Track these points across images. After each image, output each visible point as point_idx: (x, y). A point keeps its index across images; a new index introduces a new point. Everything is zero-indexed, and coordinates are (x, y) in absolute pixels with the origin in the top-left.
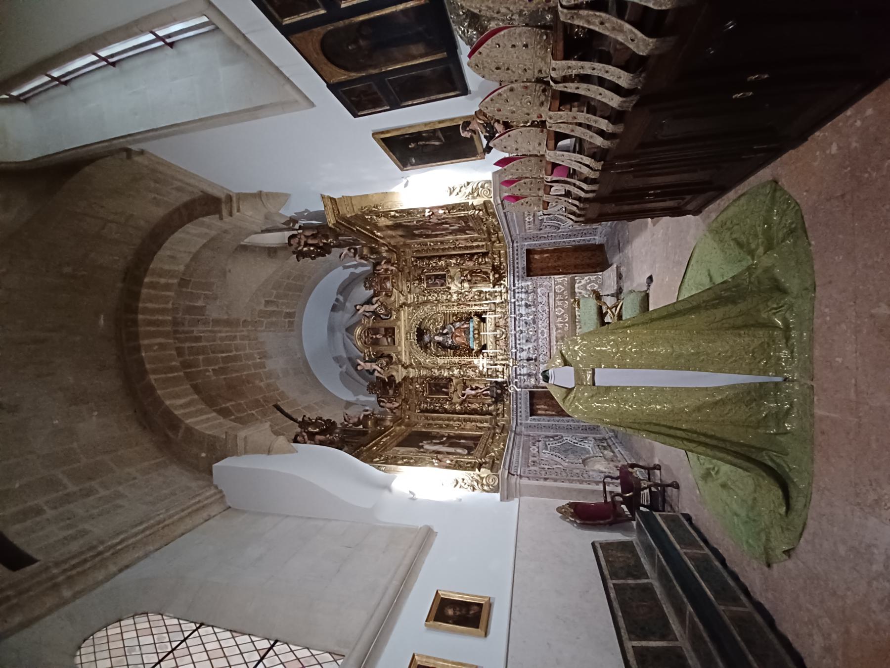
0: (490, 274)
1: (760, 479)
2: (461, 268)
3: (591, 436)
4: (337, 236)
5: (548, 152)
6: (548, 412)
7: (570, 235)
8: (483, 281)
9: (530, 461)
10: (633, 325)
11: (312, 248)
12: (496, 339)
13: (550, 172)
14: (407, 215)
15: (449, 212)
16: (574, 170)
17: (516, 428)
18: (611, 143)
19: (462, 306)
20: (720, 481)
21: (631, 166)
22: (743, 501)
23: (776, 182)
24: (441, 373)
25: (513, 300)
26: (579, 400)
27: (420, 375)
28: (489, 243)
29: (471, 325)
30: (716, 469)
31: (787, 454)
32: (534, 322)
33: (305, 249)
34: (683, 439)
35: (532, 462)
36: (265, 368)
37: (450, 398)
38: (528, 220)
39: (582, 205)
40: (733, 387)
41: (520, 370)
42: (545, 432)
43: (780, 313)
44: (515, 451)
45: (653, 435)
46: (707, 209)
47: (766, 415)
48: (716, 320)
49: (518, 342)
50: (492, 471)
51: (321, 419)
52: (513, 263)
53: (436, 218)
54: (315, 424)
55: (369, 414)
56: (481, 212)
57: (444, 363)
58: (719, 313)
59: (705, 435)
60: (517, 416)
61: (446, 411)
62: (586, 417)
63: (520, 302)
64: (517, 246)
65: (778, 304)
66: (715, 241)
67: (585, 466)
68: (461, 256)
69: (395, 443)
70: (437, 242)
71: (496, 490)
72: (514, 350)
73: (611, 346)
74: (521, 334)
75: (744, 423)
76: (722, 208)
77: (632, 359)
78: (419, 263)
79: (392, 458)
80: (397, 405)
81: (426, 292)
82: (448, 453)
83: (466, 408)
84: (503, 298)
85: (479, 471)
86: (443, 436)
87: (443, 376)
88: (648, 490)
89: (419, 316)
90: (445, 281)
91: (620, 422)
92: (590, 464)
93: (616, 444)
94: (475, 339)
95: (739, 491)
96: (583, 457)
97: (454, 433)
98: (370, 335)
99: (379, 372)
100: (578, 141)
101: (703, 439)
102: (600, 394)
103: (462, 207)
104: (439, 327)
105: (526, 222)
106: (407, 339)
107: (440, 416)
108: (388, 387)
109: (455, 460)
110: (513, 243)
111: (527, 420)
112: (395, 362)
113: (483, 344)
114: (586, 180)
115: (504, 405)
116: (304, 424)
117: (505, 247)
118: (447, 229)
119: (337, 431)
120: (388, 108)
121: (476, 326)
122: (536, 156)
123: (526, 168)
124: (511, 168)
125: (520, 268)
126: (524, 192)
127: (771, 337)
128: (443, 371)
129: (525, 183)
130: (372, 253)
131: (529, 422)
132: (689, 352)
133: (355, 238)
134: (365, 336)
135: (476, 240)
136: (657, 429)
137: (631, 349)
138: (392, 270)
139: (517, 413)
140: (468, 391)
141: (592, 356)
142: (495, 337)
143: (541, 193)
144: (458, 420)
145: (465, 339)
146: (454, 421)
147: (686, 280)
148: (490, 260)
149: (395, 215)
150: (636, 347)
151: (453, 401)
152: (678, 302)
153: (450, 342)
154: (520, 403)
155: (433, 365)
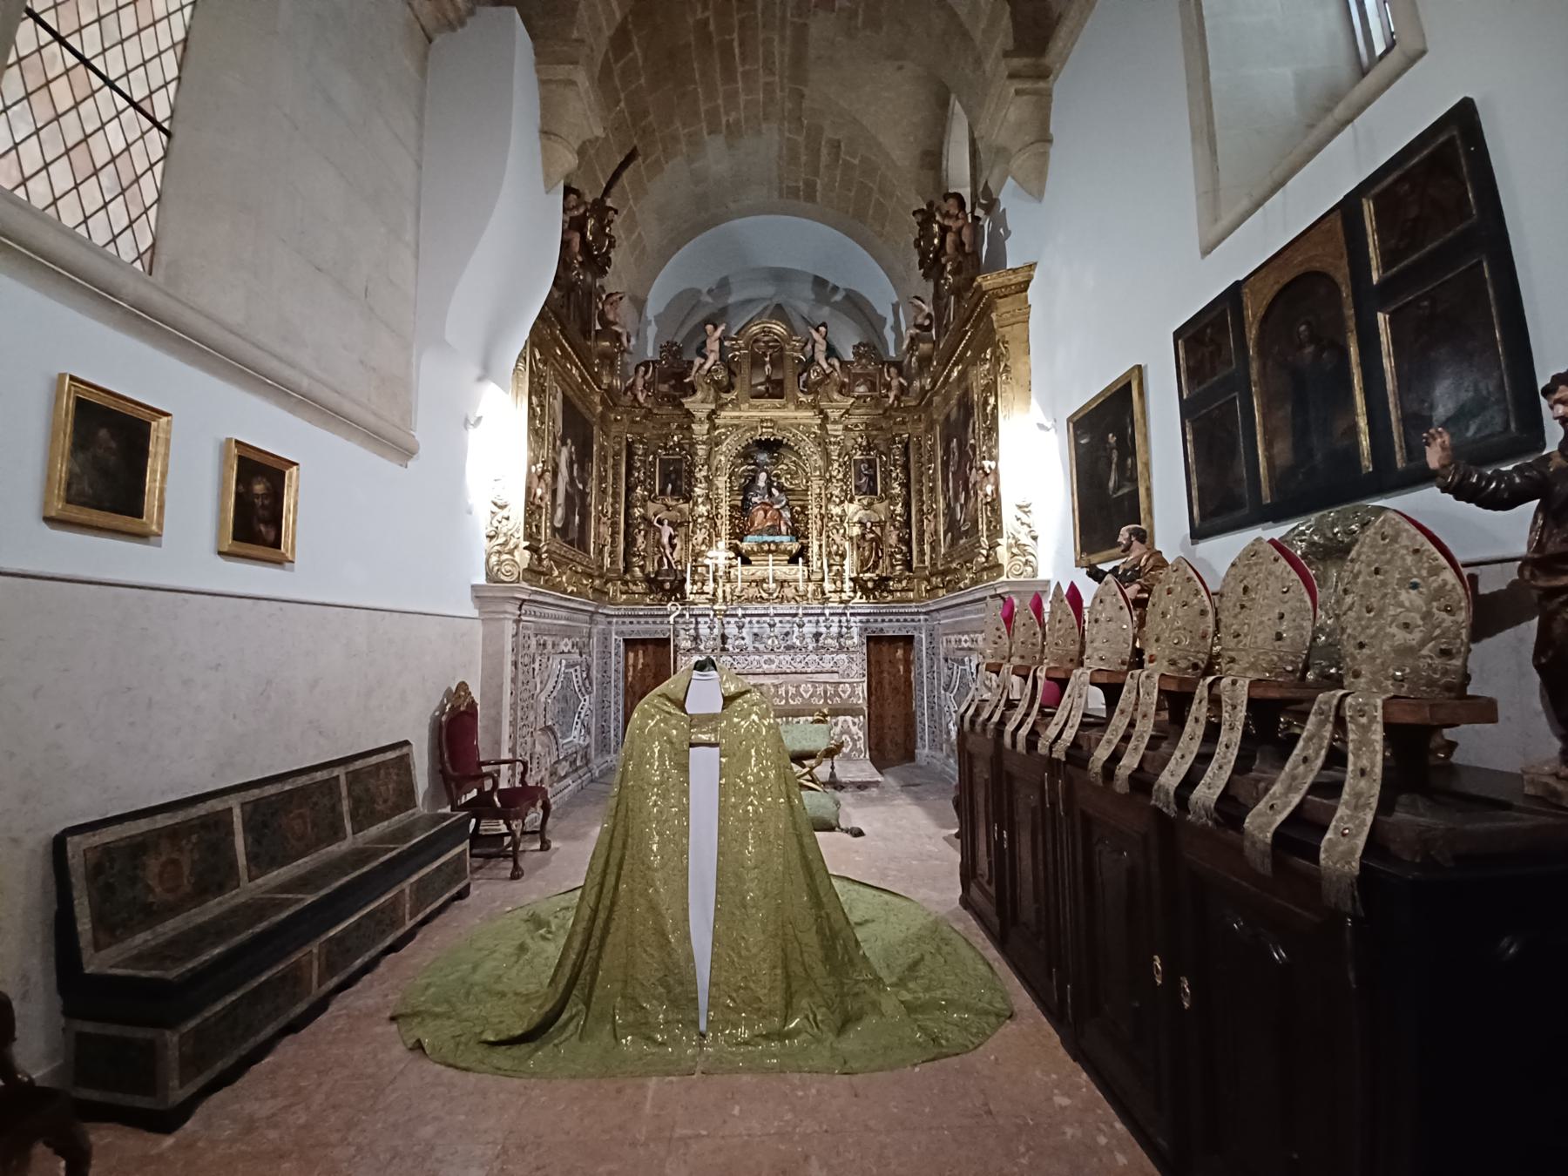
0: (873, 572)
1: (538, 1003)
2: (885, 522)
3: (591, 740)
4: (958, 292)
5: (1089, 672)
6: (631, 669)
7: (932, 708)
8: (862, 561)
9: (545, 638)
10: (792, 807)
11: (936, 241)
12: (760, 582)
13: (1052, 675)
14: (987, 427)
15: (987, 503)
16: (1053, 715)
17: (602, 614)
18: (1096, 773)
19: (820, 523)
20: (529, 941)
21: (1054, 804)
22: (500, 977)
23: (1010, 1017)
24: (701, 482)
25: (827, 612)
26: (664, 720)
27: (697, 443)
28: (927, 572)
29: (785, 539)
30: (550, 936)
31: (581, 1039)
32: (788, 648)
33: (936, 227)
34: (602, 885)
35: (545, 641)
36: (709, 134)
37: (655, 497)
38: (963, 639)
39: (992, 727)
40: (690, 958)
41: (706, 623)
42: (597, 664)
43: (807, 1025)
44: (563, 613)
45: (607, 838)
46: (971, 917)
47: (644, 1008)
48: (800, 934)
49: (755, 619)
50: (524, 570)
52: (892, 614)
53: (978, 479)
54: (600, 231)
55: (621, 344)
56: (983, 559)
57: (717, 489)
58: (811, 939)
59: (609, 920)
60: (624, 616)
61: (630, 489)
62: (634, 732)
63: (823, 624)
64: (919, 620)
65: (822, 1021)
66: (920, 929)
67: (540, 730)
68: (907, 524)
69: (570, 393)
70: (934, 481)
71: (492, 577)
72: (740, 612)
73: (758, 772)
74: (769, 624)
75: (632, 976)
76: (972, 940)
77: (735, 806)
78: (897, 449)
79: (542, 385)
80: (641, 398)
81: (847, 458)
82: (554, 493)
84: (832, 595)
85: (525, 548)
86: (585, 485)
87: (695, 486)
88: (506, 831)
89: (803, 444)
90: (865, 494)
91: (627, 787)
92: (544, 738)
93: (580, 781)
94: (760, 544)
95: (514, 971)
96: (556, 728)
97: (590, 505)
98: (771, 351)
99: (701, 366)
100: (1103, 721)
101: (602, 915)
102: (676, 754)
103: (995, 527)
104: (783, 480)
105: (960, 636)
106: (762, 421)
107: (621, 479)
108: (673, 382)
109: (544, 505)
110: (925, 613)
111: (616, 634)
112: (721, 397)
113: (751, 558)
114: (1034, 734)
116: (600, 210)
117: (919, 600)
118: (957, 498)
119: (589, 279)
120: (1185, 397)
121: (782, 547)
122: (1082, 652)
123: (1062, 636)
124: (1063, 611)
125: (881, 625)
126: (1020, 635)
127: (771, 1013)
128: (703, 485)
129: (1034, 634)
130: (920, 360)
131: (614, 637)
132: (748, 892)
133: (951, 327)
134: (768, 342)
135: (933, 549)
136: (618, 843)
137: (751, 804)
138: (887, 397)
139: (630, 616)
140: (667, 531)
141: (741, 744)
142: (764, 581)
143: (1016, 660)
144: (615, 513)
145: (760, 527)
146: (612, 505)
147: (856, 887)
148: (898, 573)
149: (989, 404)
150: (756, 811)
151: (649, 503)
152: (829, 876)
153: (755, 499)
154: (647, 623)
155: (714, 469)
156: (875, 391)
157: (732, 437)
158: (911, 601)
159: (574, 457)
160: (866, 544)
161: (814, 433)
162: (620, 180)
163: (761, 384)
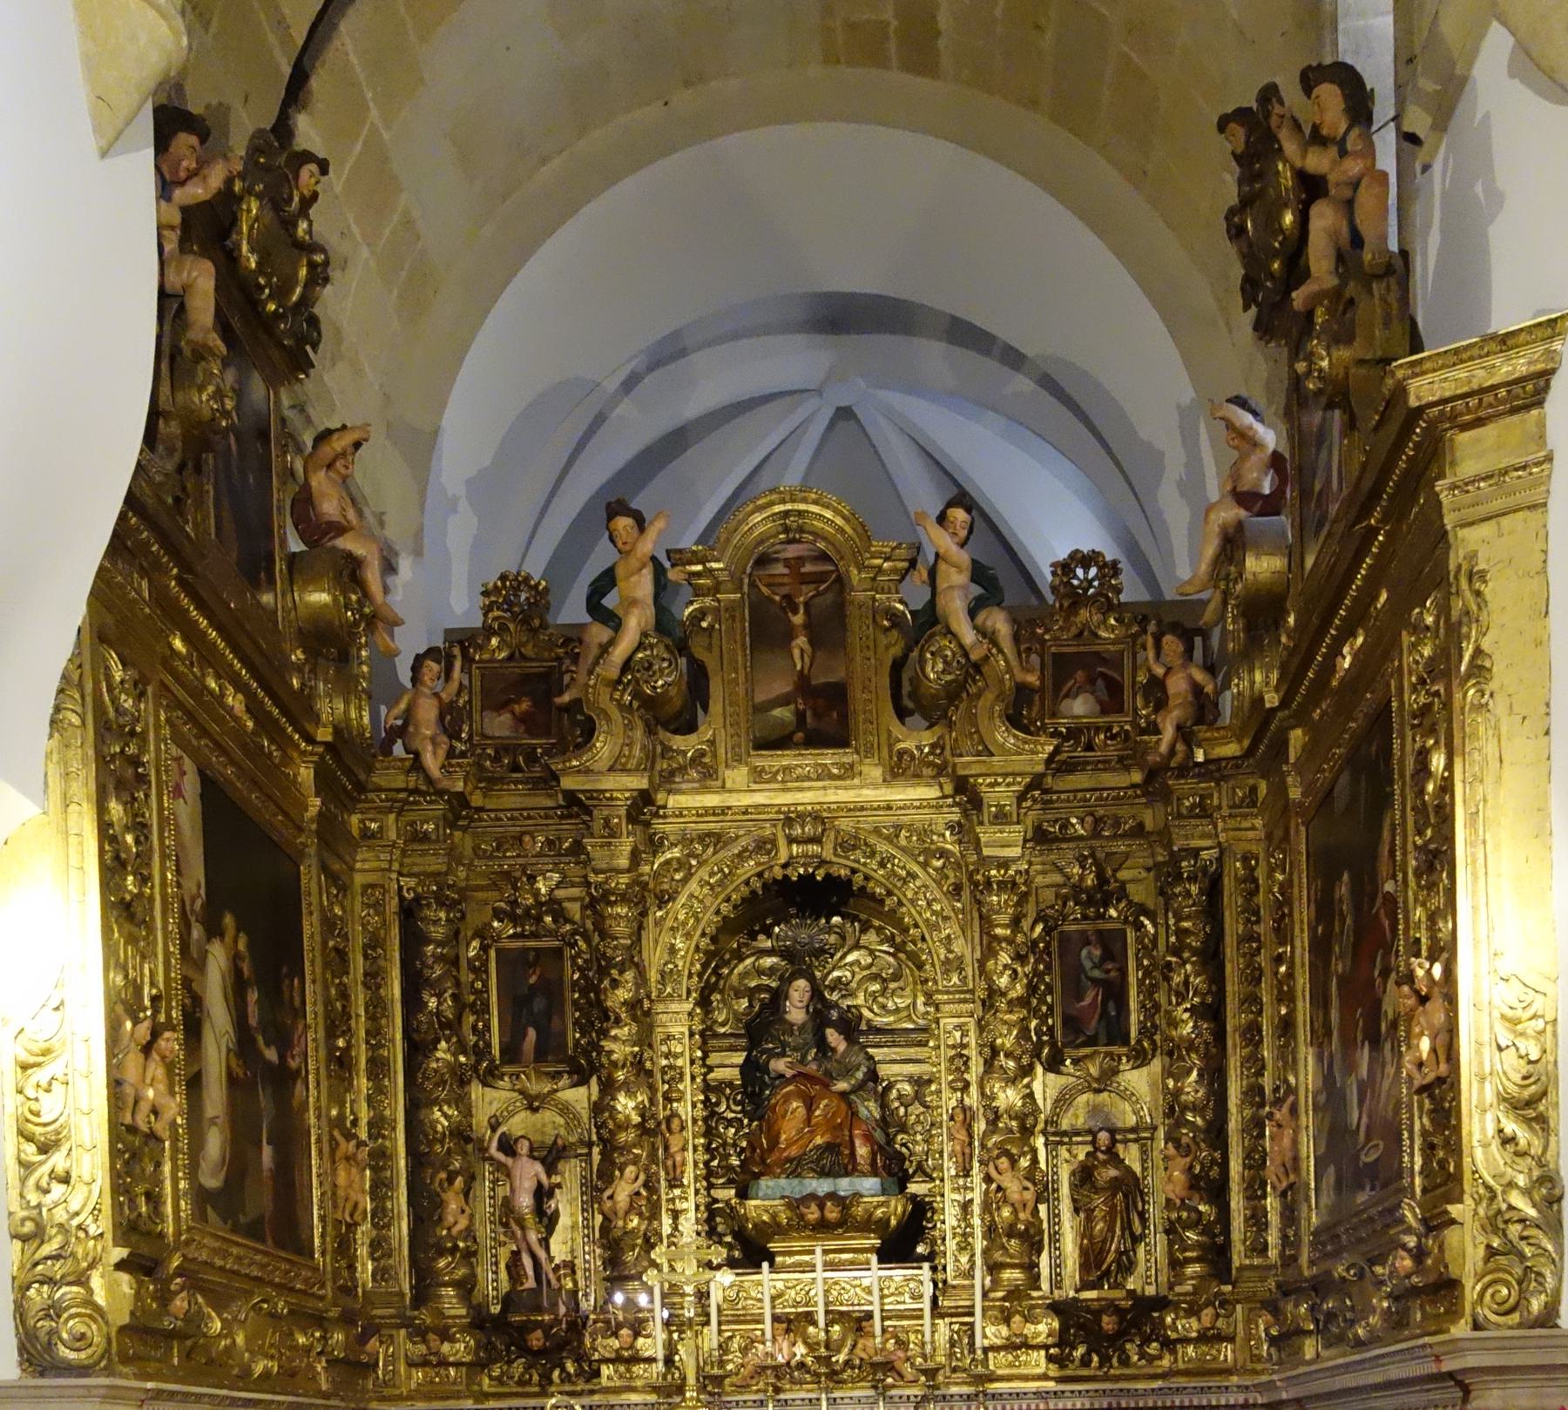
24: (618, 1021)
51: (319, 277)
61: (417, 1050)
82: (194, 1084)
83: (445, 1167)
94: (795, 1204)
99: (605, 649)
115: (469, 1365)
121: (859, 1211)
134: (800, 560)
135: (1290, 1216)
138: (1155, 730)
140: (529, 1172)
145: (794, 1152)
151: (476, 1091)
153: (779, 1065)
156: (1120, 710)
157: (703, 873)
158: (1227, 1372)
159: (246, 968)
160: (1098, 1200)
161: (943, 854)
162: (336, 43)
163: (784, 701)
